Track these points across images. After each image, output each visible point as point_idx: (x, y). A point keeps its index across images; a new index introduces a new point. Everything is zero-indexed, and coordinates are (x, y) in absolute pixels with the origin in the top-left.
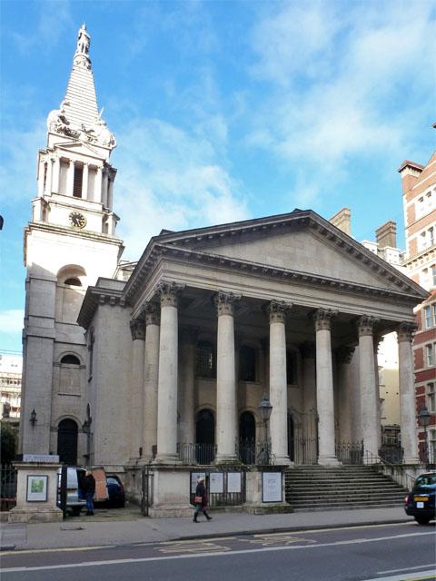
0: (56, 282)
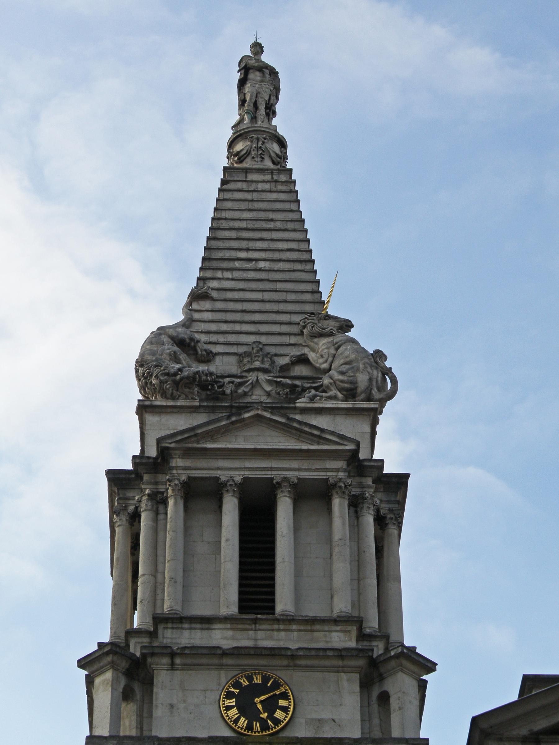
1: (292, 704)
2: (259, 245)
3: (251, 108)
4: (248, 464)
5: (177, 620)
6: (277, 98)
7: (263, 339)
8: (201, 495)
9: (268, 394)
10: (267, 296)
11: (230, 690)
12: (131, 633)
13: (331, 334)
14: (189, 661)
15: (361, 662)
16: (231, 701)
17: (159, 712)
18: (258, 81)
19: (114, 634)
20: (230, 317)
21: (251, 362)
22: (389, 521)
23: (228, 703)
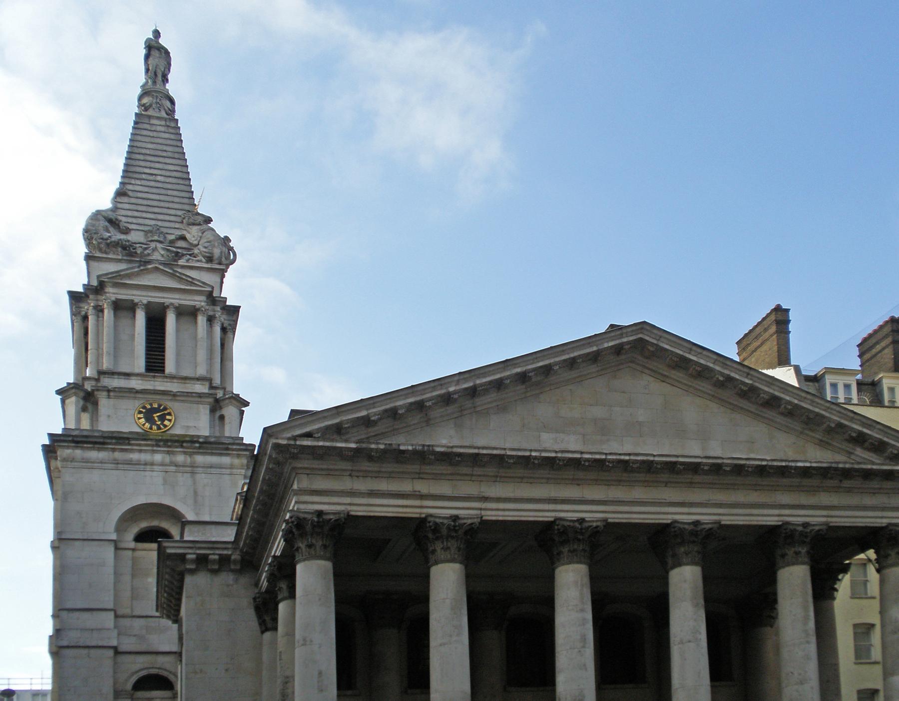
0: (115, 542)
2: (157, 165)
3: (153, 75)
4: (150, 294)
5: (112, 374)
6: (169, 70)
7: (160, 223)
8: (124, 308)
9: (162, 256)
10: (162, 198)
12: (85, 379)
13: (199, 224)
14: (118, 394)
15: (211, 400)
17: (102, 419)
18: (156, 53)
19: (76, 378)
20: (140, 208)
21: (152, 236)
22: (228, 330)
23: (139, 416)
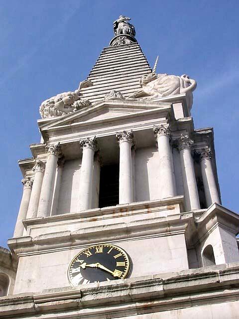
1: (128, 264)
11: (77, 261)
16: (77, 269)
23: (74, 271)
